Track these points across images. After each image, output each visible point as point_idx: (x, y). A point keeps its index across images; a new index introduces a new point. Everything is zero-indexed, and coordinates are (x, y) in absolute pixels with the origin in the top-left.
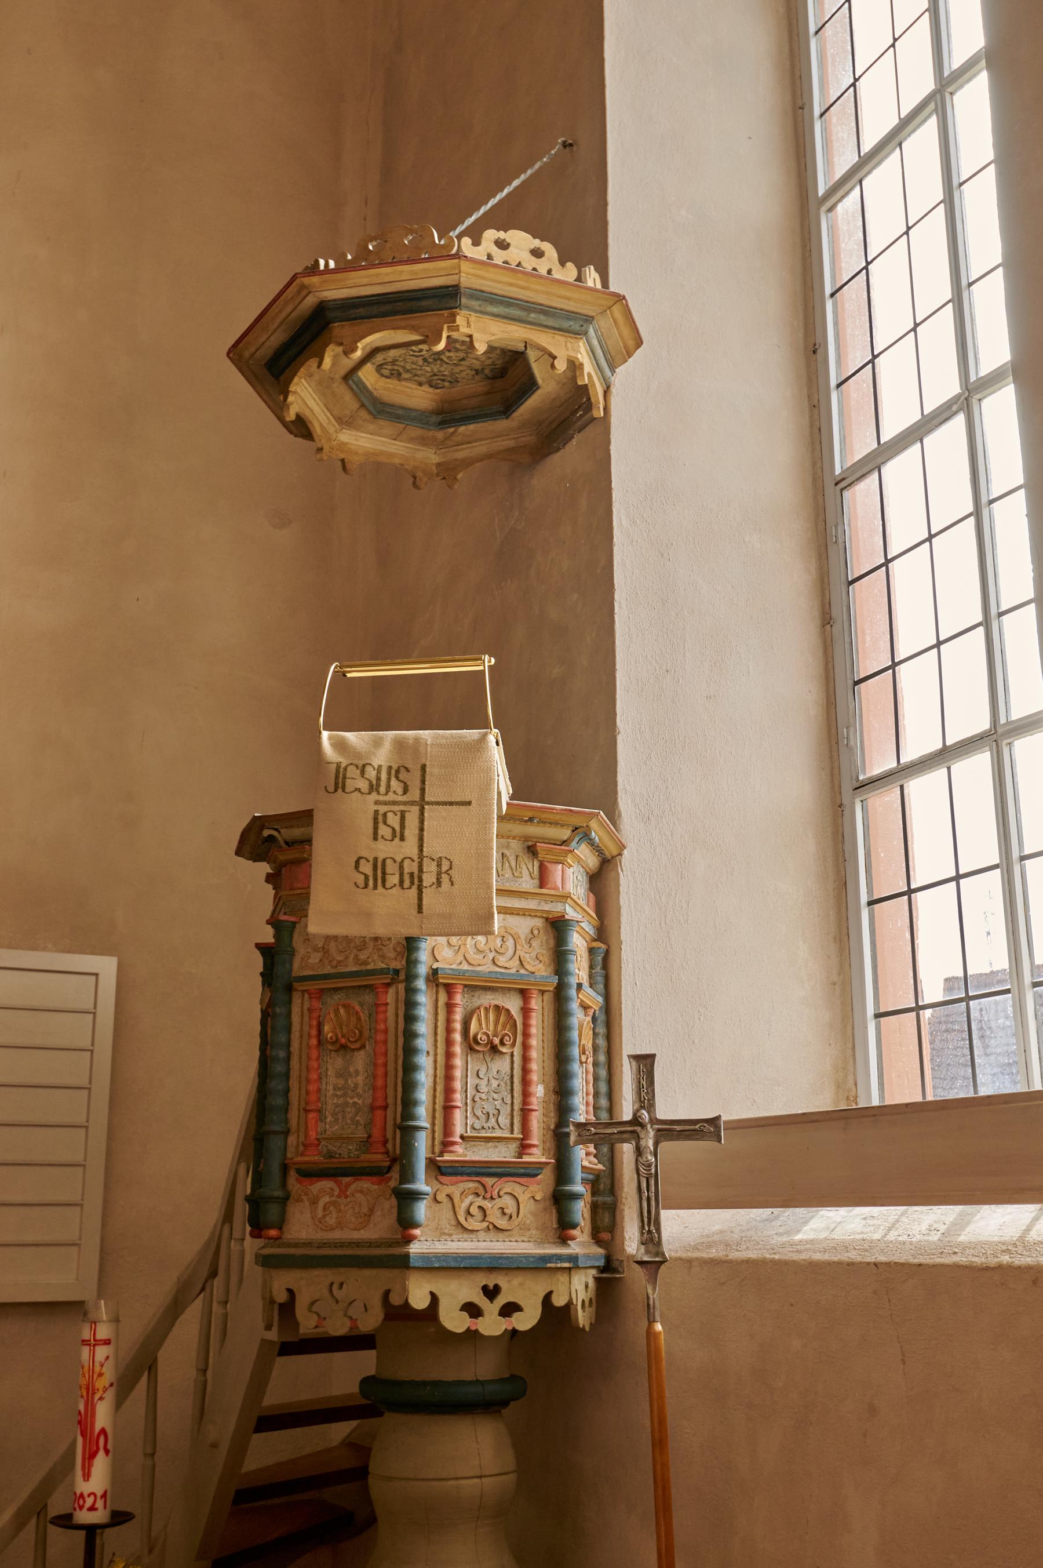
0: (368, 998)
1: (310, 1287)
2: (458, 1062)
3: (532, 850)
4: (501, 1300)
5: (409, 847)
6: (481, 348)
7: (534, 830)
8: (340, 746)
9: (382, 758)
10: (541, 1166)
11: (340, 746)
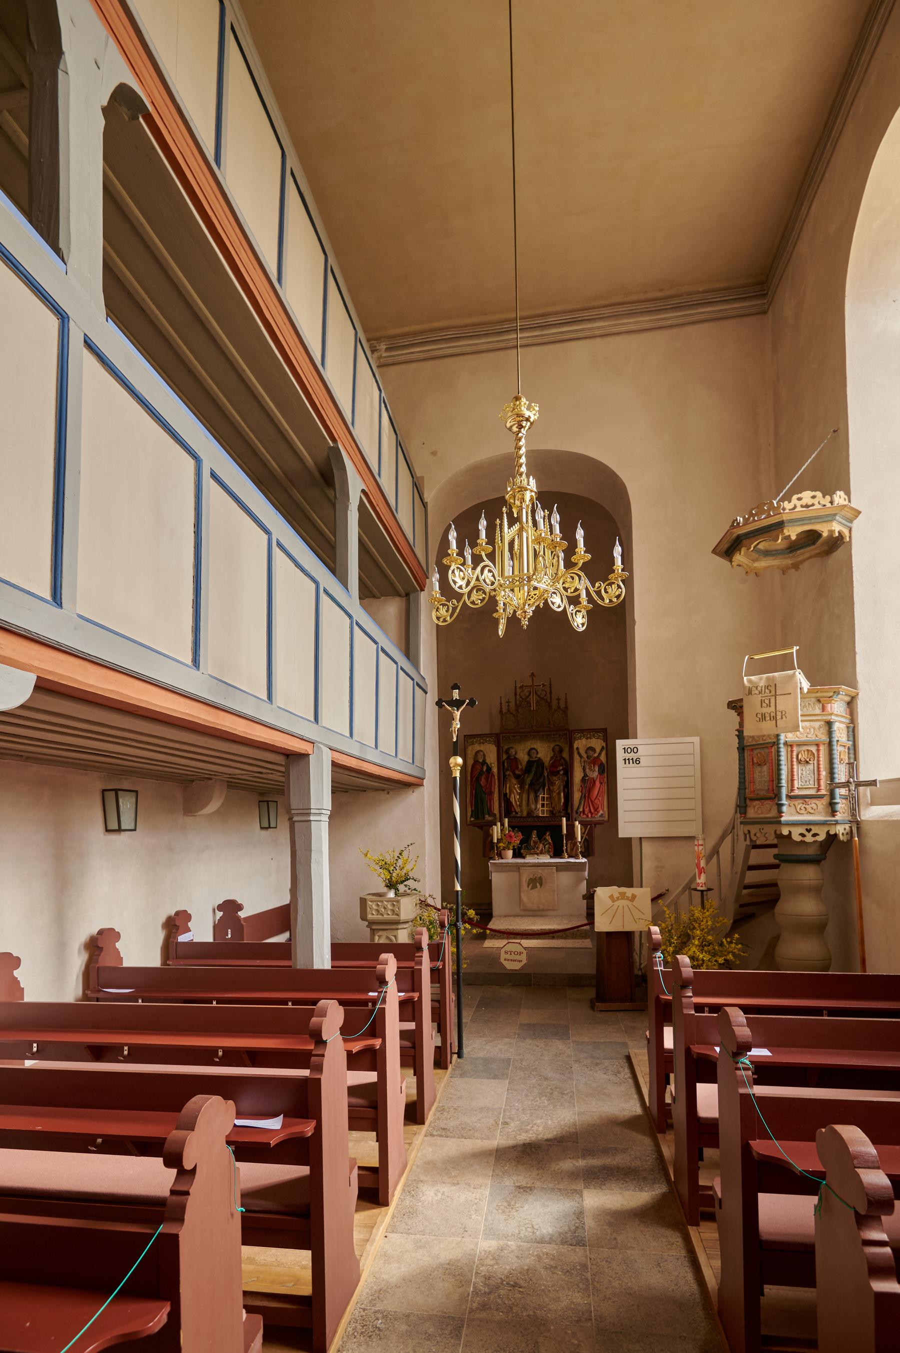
0: (767, 751)
1: (754, 829)
2: (795, 767)
3: (819, 701)
4: (812, 833)
5: (772, 709)
6: (793, 538)
7: (819, 694)
8: (750, 681)
9: (762, 683)
10: (824, 795)
11: (750, 681)
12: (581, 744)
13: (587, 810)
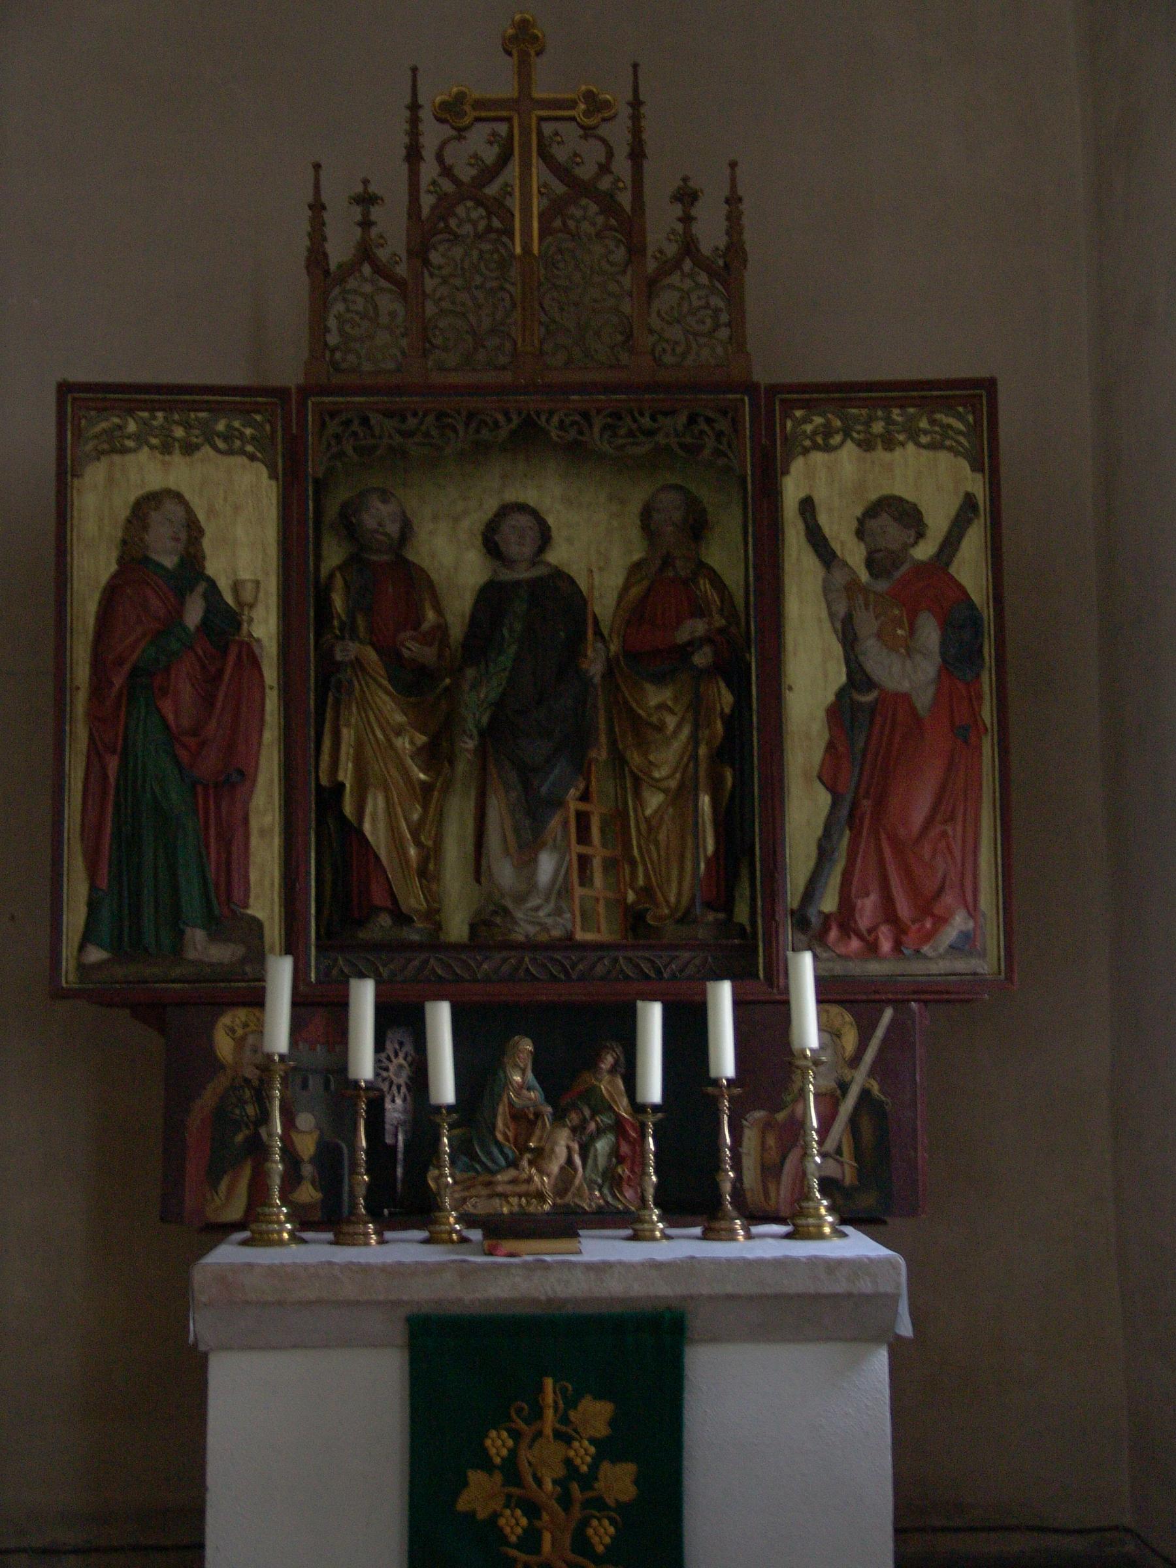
12: (828, 480)
13: (867, 908)
